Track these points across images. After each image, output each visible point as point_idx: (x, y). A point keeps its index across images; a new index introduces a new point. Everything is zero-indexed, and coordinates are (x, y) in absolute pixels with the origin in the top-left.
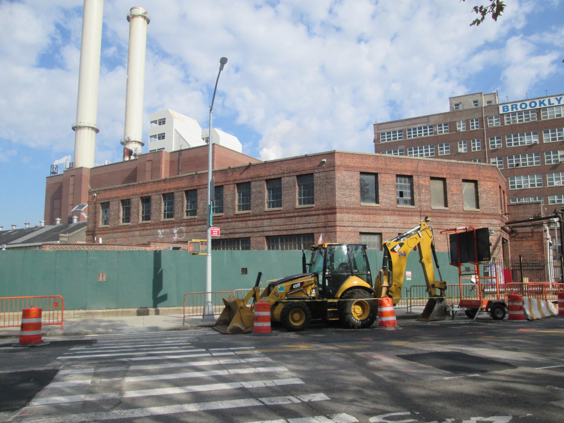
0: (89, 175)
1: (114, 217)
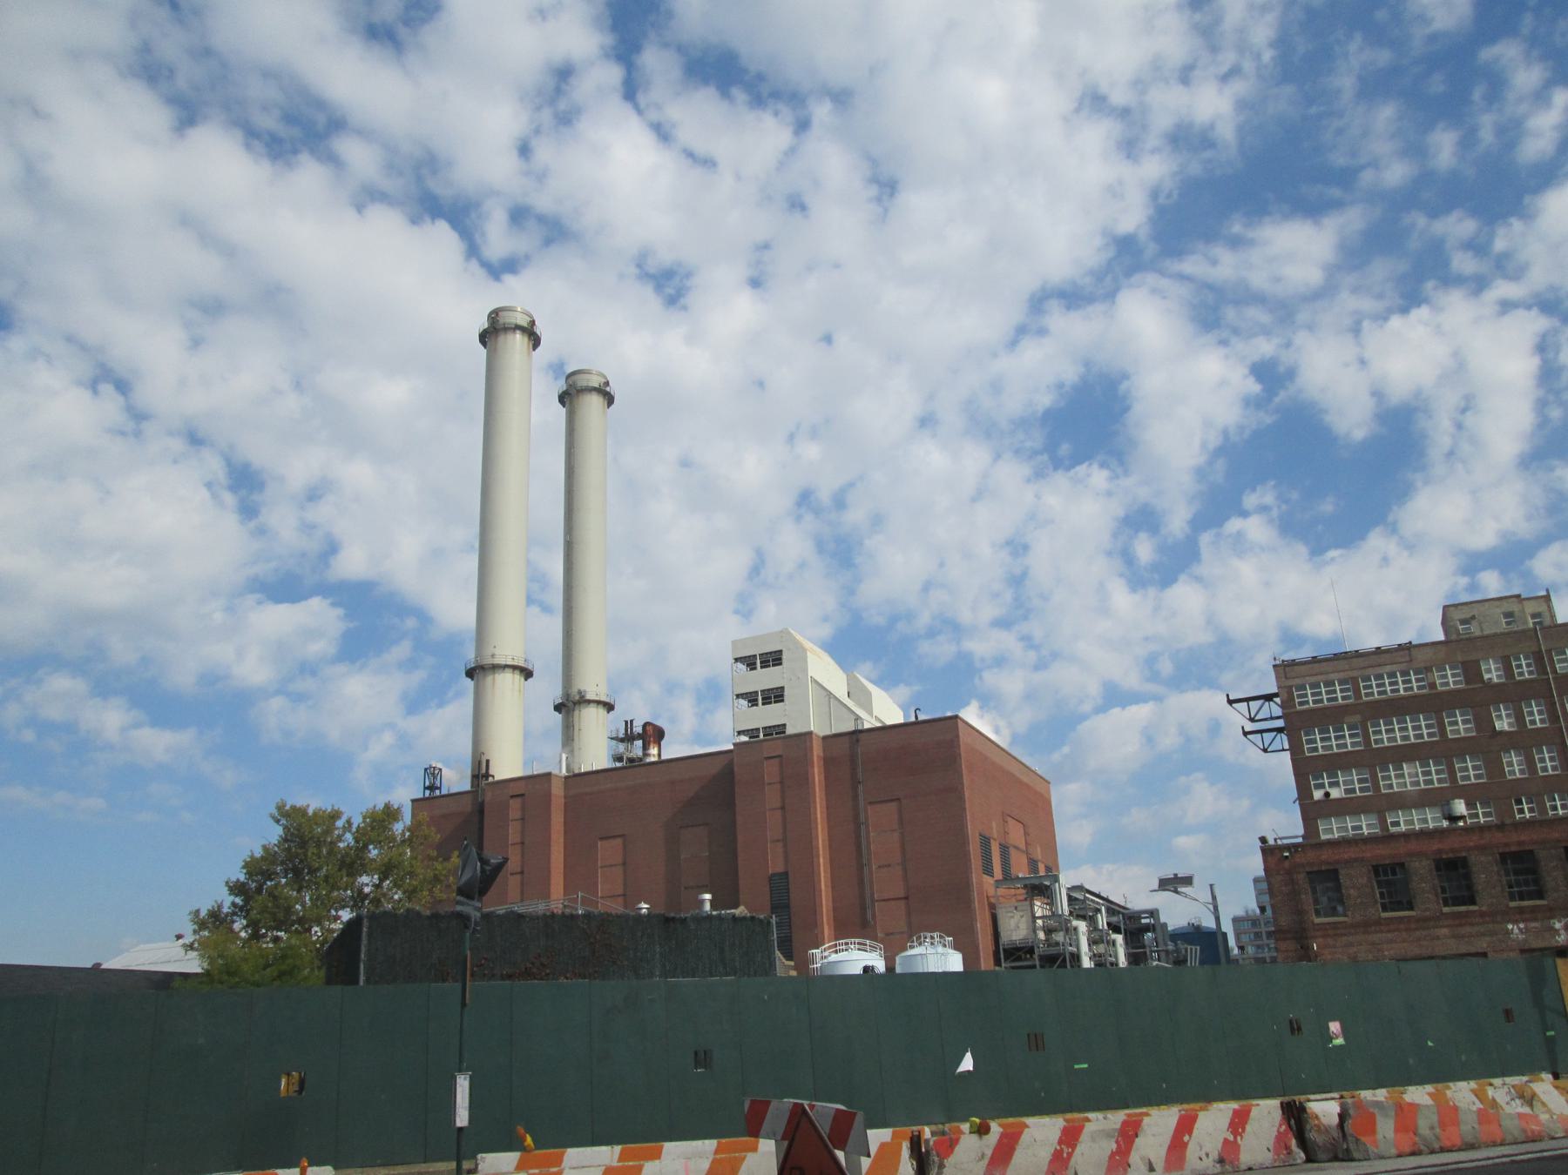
0: (563, 794)
1: (1359, 900)
